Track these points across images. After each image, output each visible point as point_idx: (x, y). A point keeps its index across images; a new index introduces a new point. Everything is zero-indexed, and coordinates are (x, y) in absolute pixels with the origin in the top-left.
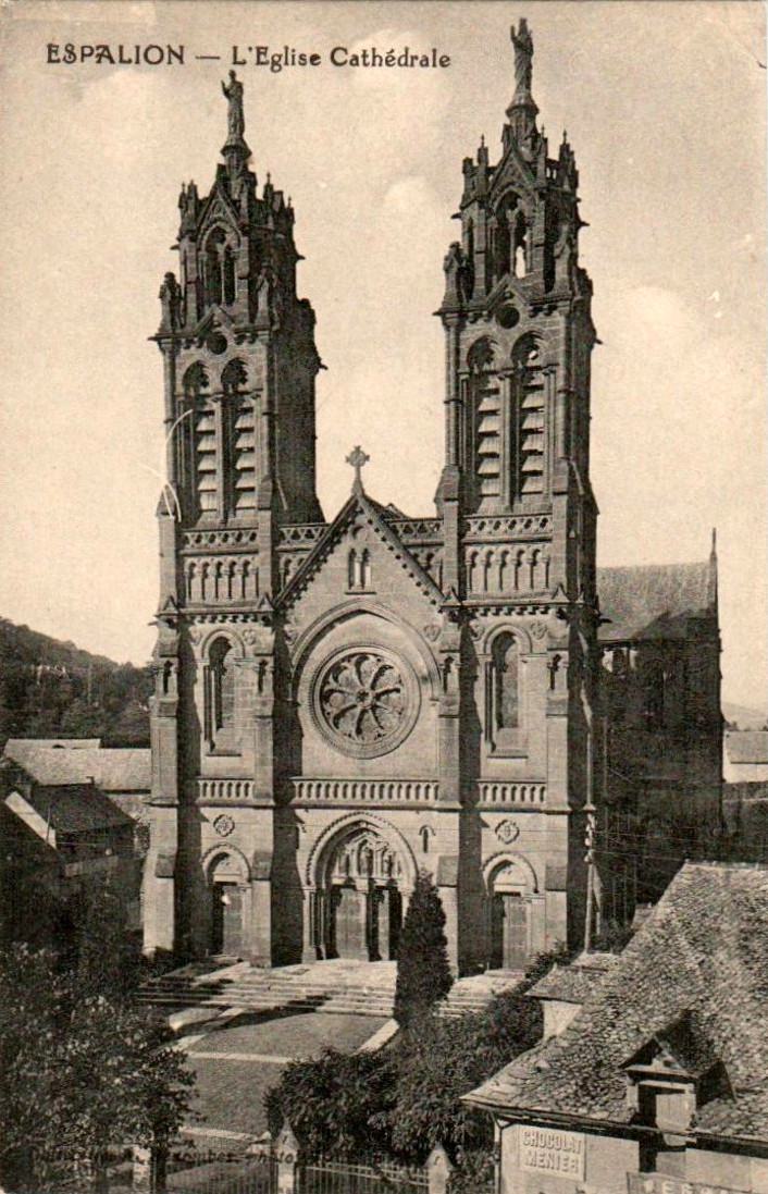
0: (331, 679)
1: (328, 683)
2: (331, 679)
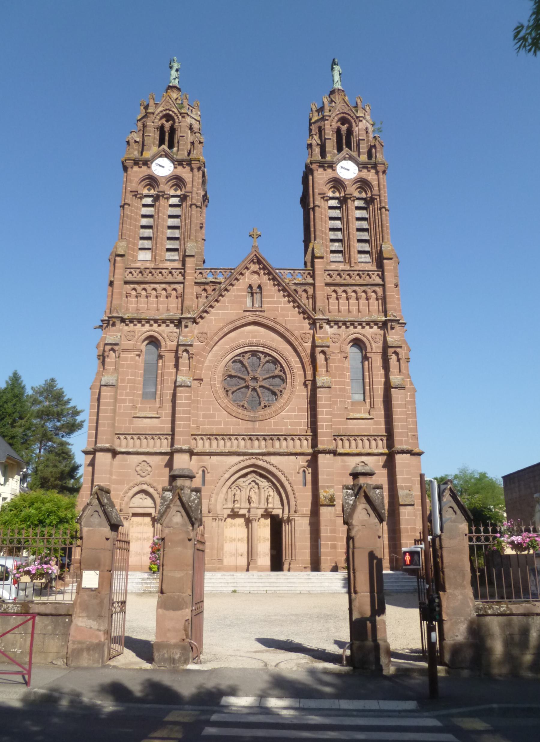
1: (265, 357)
2: (268, 358)
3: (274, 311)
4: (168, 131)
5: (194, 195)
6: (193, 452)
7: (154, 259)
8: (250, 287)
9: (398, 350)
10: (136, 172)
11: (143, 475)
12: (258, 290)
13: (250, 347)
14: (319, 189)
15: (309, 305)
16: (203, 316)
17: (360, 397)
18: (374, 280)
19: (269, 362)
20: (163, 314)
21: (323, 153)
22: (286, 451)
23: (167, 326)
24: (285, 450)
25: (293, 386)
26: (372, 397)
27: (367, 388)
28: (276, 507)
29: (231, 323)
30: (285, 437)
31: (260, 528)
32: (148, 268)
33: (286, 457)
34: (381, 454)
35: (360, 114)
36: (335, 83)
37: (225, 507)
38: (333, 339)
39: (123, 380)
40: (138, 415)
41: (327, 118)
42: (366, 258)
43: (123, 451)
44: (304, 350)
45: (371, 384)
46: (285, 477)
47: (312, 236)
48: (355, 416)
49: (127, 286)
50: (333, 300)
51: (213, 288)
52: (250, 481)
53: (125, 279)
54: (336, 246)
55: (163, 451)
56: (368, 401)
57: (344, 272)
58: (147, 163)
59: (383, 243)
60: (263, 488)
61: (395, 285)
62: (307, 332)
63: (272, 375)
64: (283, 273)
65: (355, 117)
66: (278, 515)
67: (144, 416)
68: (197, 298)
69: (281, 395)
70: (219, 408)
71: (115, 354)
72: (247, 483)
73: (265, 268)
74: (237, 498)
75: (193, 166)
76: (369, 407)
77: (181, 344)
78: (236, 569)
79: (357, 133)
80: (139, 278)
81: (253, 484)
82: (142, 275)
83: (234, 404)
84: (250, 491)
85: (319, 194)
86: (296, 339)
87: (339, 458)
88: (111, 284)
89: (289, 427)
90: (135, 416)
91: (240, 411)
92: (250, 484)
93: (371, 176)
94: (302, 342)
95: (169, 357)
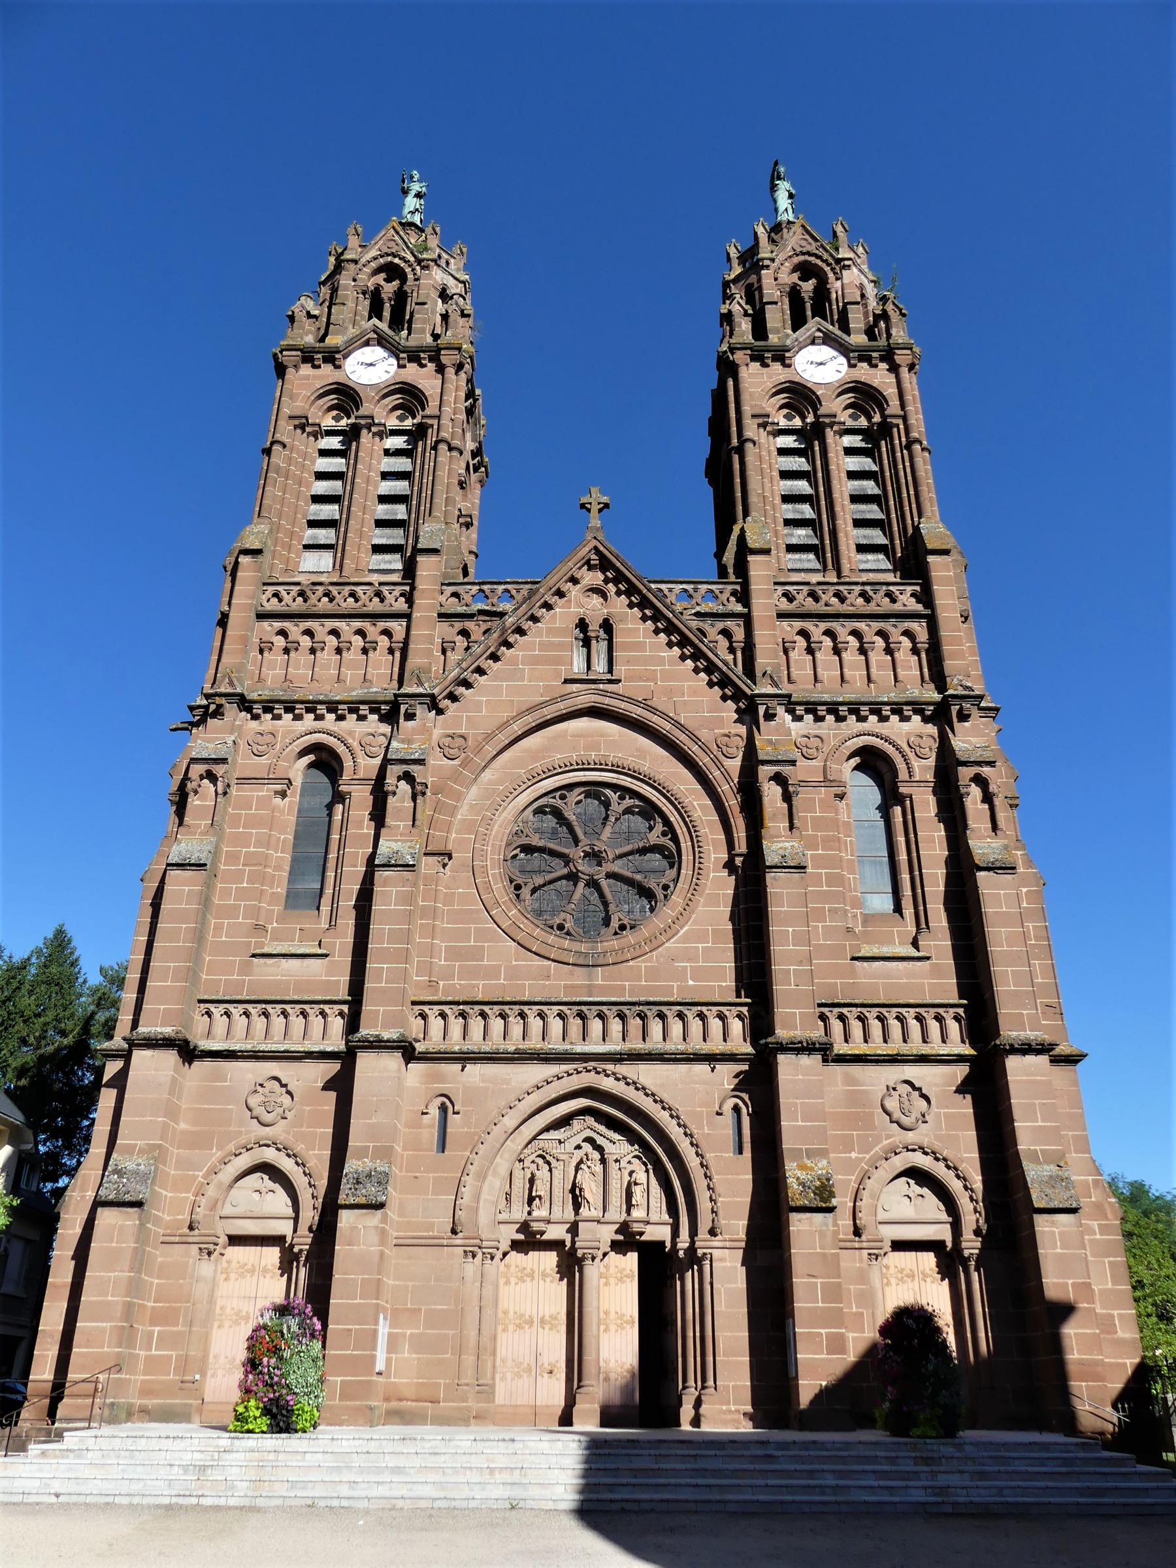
0: (628, 802)
1: (622, 798)
2: (628, 802)
3: (645, 681)
4: (390, 299)
5: (445, 421)
6: (414, 1049)
7: (340, 566)
8: (582, 625)
9: (986, 771)
10: (307, 377)
11: (268, 1118)
12: (602, 634)
13: (582, 773)
14: (752, 407)
15: (735, 665)
16: (456, 693)
17: (885, 903)
18: (905, 605)
19: (633, 813)
20: (354, 689)
21: (760, 330)
22: (682, 1047)
23: (362, 718)
24: (679, 1047)
25: (697, 870)
26: (919, 901)
27: (905, 877)
28: (654, 1217)
29: (531, 709)
30: (679, 1008)
31: (606, 1284)
32: (320, 584)
33: (683, 1068)
34: (960, 1059)
35: (844, 253)
36: (779, 213)
37: (504, 1216)
38: (805, 750)
39: (233, 857)
40: (266, 950)
41: (766, 262)
42: (878, 560)
43: (214, 1049)
44: (726, 775)
45: (915, 864)
46: (679, 1125)
47: (740, 508)
48: (875, 951)
49: (265, 624)
50: (798, 654)
51: (484, 627)
52: (578, 1140)
53: (260, 608)
54: (801, 535)
55: (329, 1049)
56: (909, 912)
57: (825, 587)
58: (332, 357)
59: (922, 520)
60: (617, 1161)
61: (962, 616)
62: (733, 731)
63: (641, 845)
64: (666, 591)
65: (831, 261)
66: (662, 1244)
67: (283, 952)
68: (444, 651)
69: (666, 896)
70: (495, 931)
71: (215, 785)
72: (570, 1146)
73: (619, 578)
74: (541, 1189)
75: (445, 360)
76: (914, 929)
77: (394, 757)
78: (531, 1417)
79: (840, 293)
80: (298, 605)
81: (587, 1147)
82: (305, 601)
83: (536, 921)
84: (577, 1168)
85: (754, 416)
86: (705, 748)
87: (838, 1070)
88: (223, 621)
89: (691, 982)
90: (258, 951)
91: (551, 939)
92: (578, 1147)
93: (879, 377)
94: (722, 758)
95: (361, 797)
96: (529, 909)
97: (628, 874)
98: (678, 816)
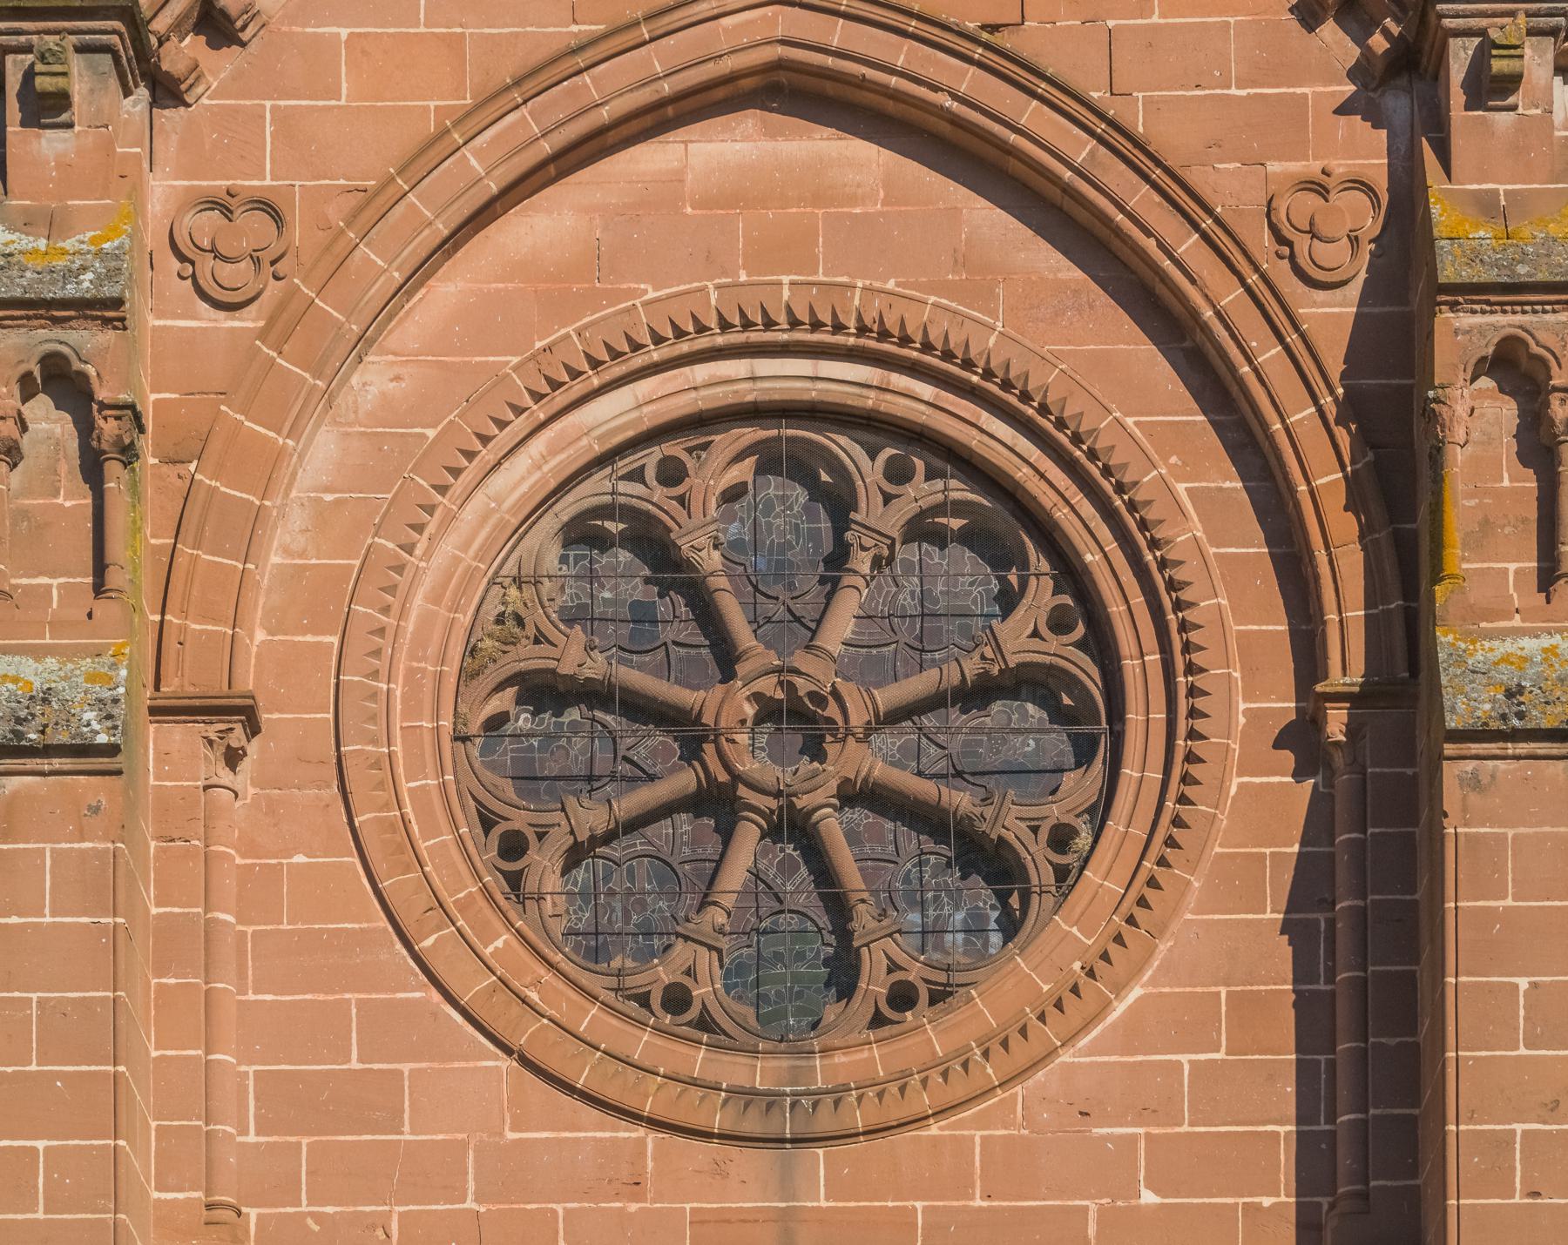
1: (898, 473)
2: (921, 492)
19: (939, 538)
63: (972, 667)
69: (1061, 873)
83: (585, 979)
96: (558, 927)
97: (926, 789)
98: (1112, 546)
